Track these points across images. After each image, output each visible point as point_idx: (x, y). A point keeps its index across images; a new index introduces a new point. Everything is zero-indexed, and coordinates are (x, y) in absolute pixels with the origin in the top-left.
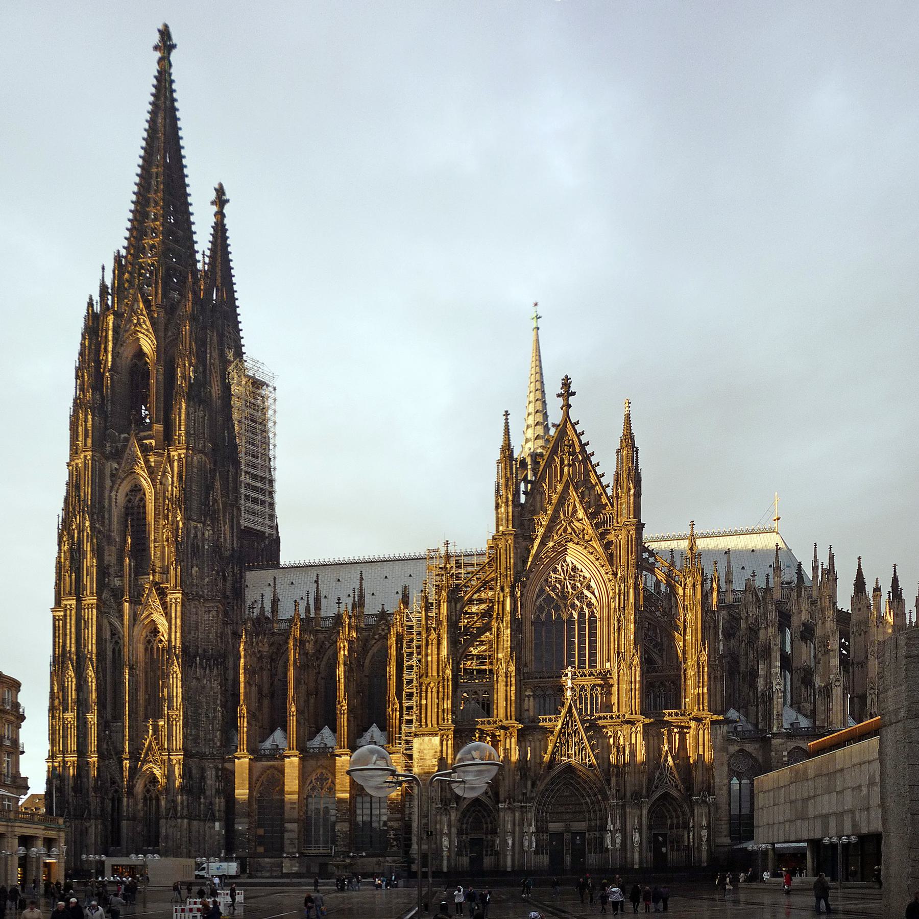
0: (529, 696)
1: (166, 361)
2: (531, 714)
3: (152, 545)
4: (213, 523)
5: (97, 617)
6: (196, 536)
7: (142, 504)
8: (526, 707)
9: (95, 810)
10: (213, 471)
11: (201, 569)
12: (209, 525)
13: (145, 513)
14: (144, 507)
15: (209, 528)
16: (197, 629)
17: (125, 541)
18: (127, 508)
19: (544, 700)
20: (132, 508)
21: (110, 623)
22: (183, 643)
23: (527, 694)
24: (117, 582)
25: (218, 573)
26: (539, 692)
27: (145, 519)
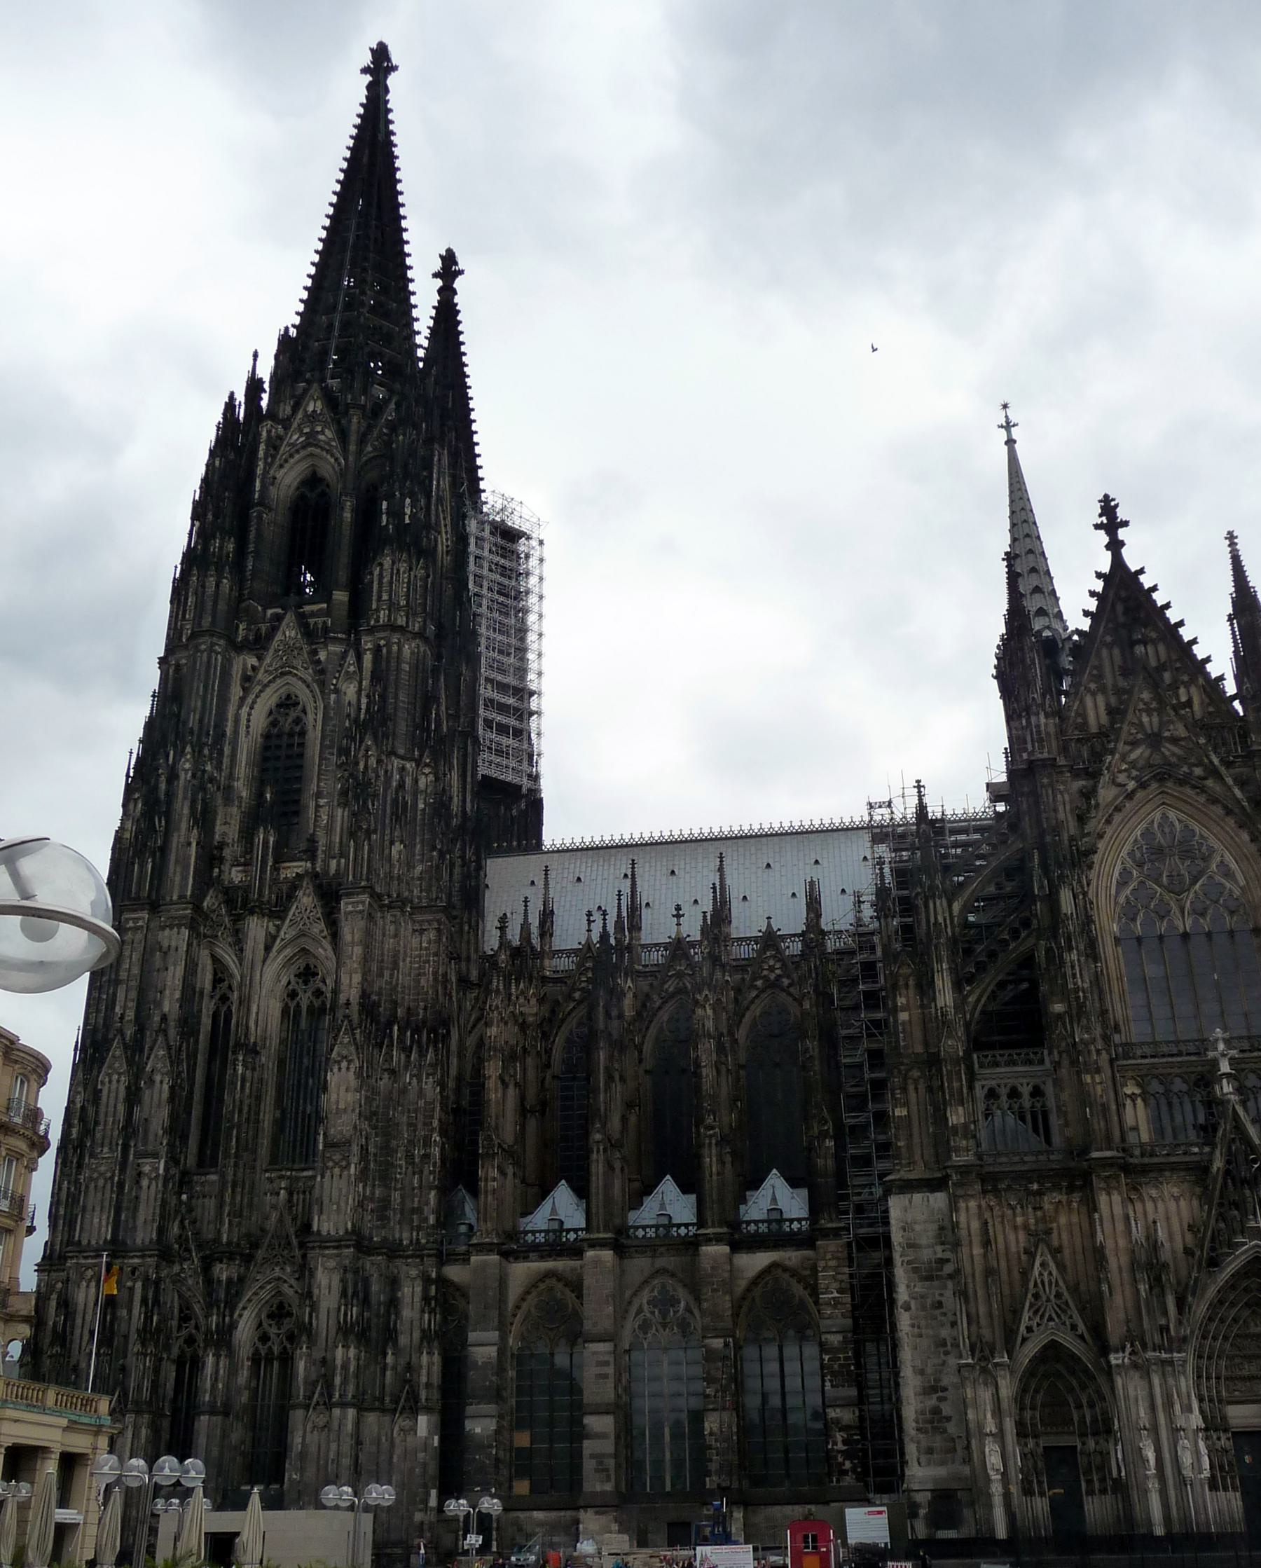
0: (1133, 1097)
1: (351, 496)
2: (1145, 1137)
3: (312, 804)
4: (435, 760)
5: (189, 945)
6: (401, 785)
7: (298, 729)
8: (1129, 1120)
9: (139, 1388)
10: (435, 671)
11: (409, 847)
12: (427, 765)
13: (302, 745)
14: (303, 733)
15: (427, 770)
16: (395, 966)
17: (261, 795)
18: (267, 736)
19: (1170, 1104)
20: (279, 736)
21: (215, 960)
22: (364, 995)
23: (1129, 1092)
24: (236, 875)
25: (442, 854)
26: (1155, 1086)
27: (301, 755)
